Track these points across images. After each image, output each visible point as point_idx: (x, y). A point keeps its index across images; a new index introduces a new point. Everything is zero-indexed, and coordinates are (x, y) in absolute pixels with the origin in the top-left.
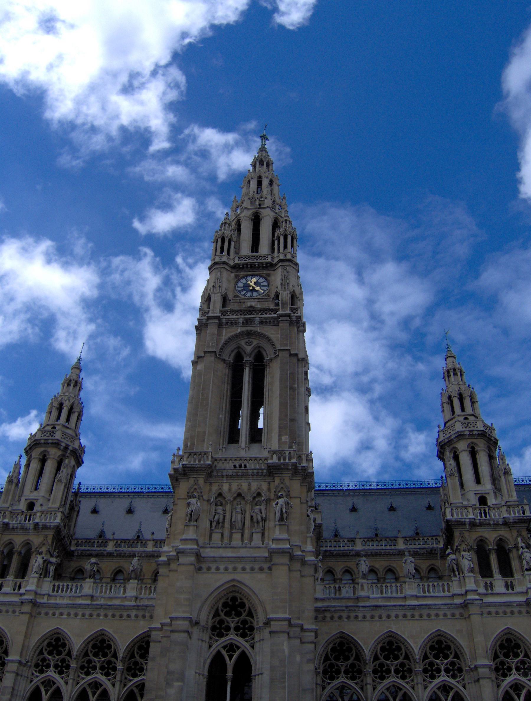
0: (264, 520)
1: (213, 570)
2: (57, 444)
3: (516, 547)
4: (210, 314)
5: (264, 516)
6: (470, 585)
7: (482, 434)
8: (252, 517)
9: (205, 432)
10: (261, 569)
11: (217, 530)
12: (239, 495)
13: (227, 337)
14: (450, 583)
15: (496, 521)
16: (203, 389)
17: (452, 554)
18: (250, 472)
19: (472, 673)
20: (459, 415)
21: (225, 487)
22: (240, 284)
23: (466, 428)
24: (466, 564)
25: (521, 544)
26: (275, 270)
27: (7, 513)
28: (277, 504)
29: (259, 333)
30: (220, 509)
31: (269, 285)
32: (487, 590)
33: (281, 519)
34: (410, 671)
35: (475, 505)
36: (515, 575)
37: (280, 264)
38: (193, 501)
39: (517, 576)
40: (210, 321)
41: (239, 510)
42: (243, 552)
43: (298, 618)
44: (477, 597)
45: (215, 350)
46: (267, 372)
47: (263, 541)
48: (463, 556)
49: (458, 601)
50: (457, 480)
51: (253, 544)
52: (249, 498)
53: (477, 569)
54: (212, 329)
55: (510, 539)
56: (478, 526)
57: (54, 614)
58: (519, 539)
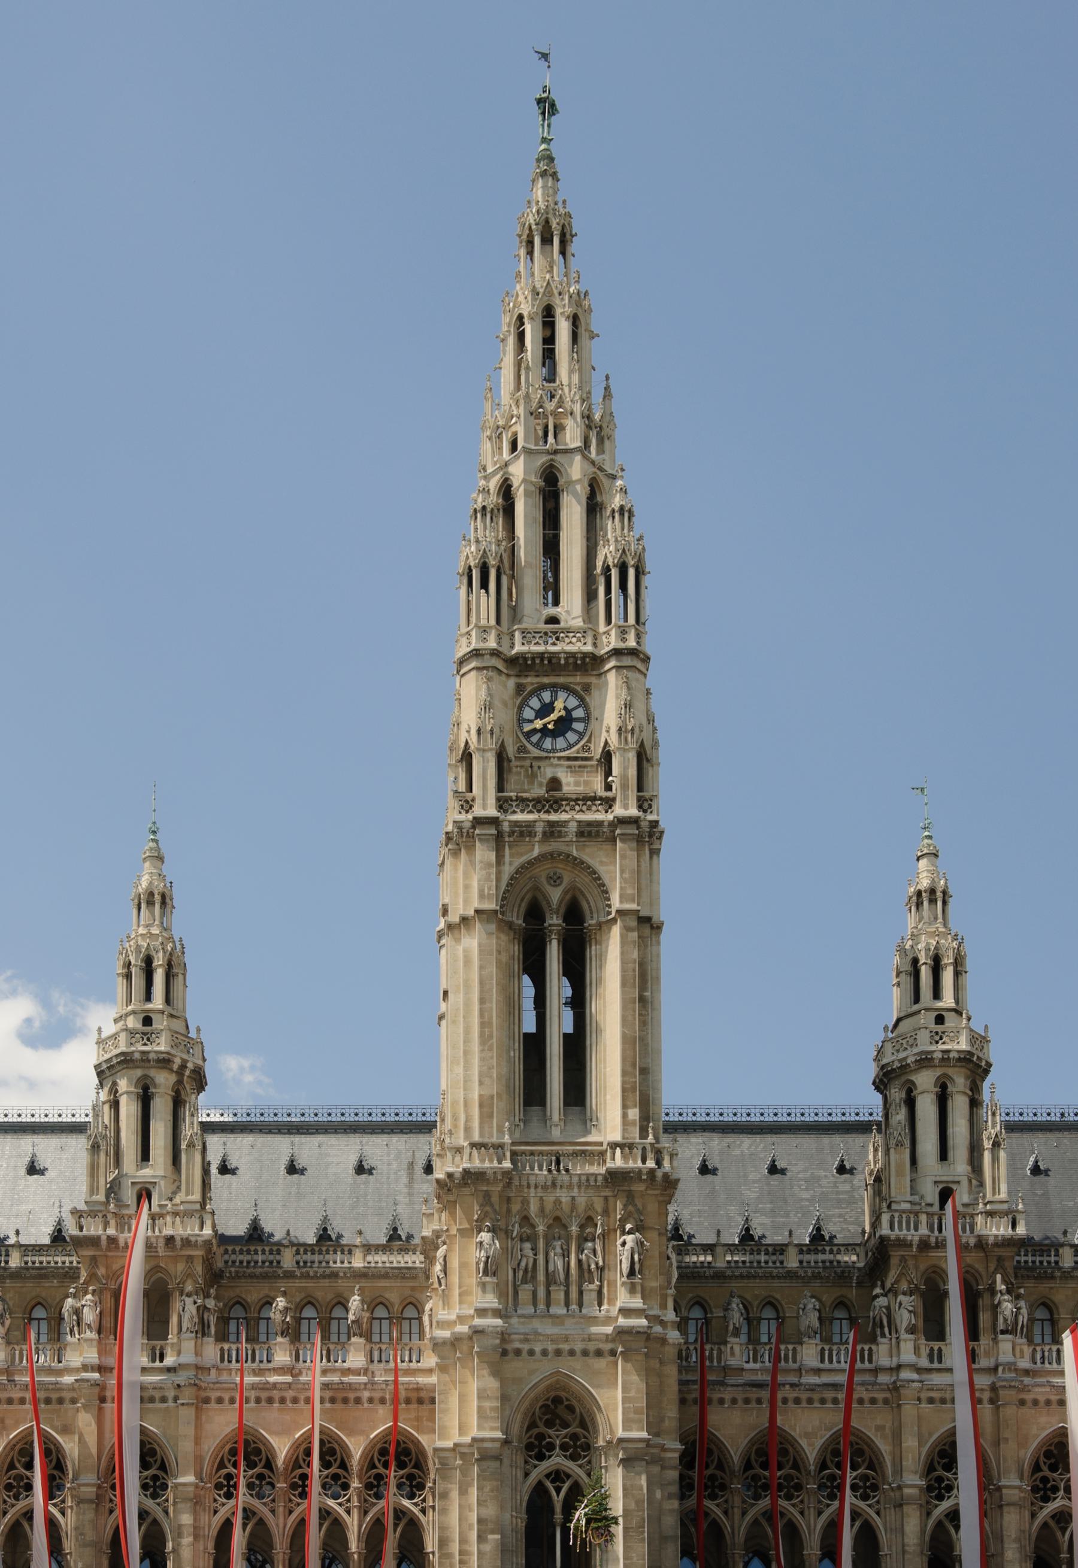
0: (602, 1269)
1: (524, 1353)
3: (992, 1290)
4: (478, 811)
5: (601, 1263)
6: (907, 1355)
7: (965, 1058)
8: (580, 1261)
9: (492, 1097)
10: (599, 1353)
11: (526, 1286)
12: (557, 1219)
13: (513, 869)
14: (874, 1347)
15: (964, 1240)
16: (482, 1001)
17: (882, 1295)
18: (575, 1180)
19: (892, 1494)
20: (926, 1010)
21: (533, 1208)
22: (528, 714)
23: (937, 1042)
24: (904, 1318)
25: (1001, 1286)
29: (575, 859)
30: (527, 1246)
32: (932, 1361)
34: (799, 1487)
35: (931, 1205)
36: (982, 1337)
38: (485, 1236)
39: (985, 1341)
41: (559, 1250)
43: (657, 1434)
44: (915, 1376)
45: (492, 905)
46: (592, 951)
47: (600, 1304)
48: (900, 1304)
49: (884, 1378)
50: (908, 1151)
51: (584, 1311)
52: (574, 1229)
53: (921, 1324)
54: (484, 853)
55: (984, 1273)
56: (933, 1248)
58: (999, 1277)
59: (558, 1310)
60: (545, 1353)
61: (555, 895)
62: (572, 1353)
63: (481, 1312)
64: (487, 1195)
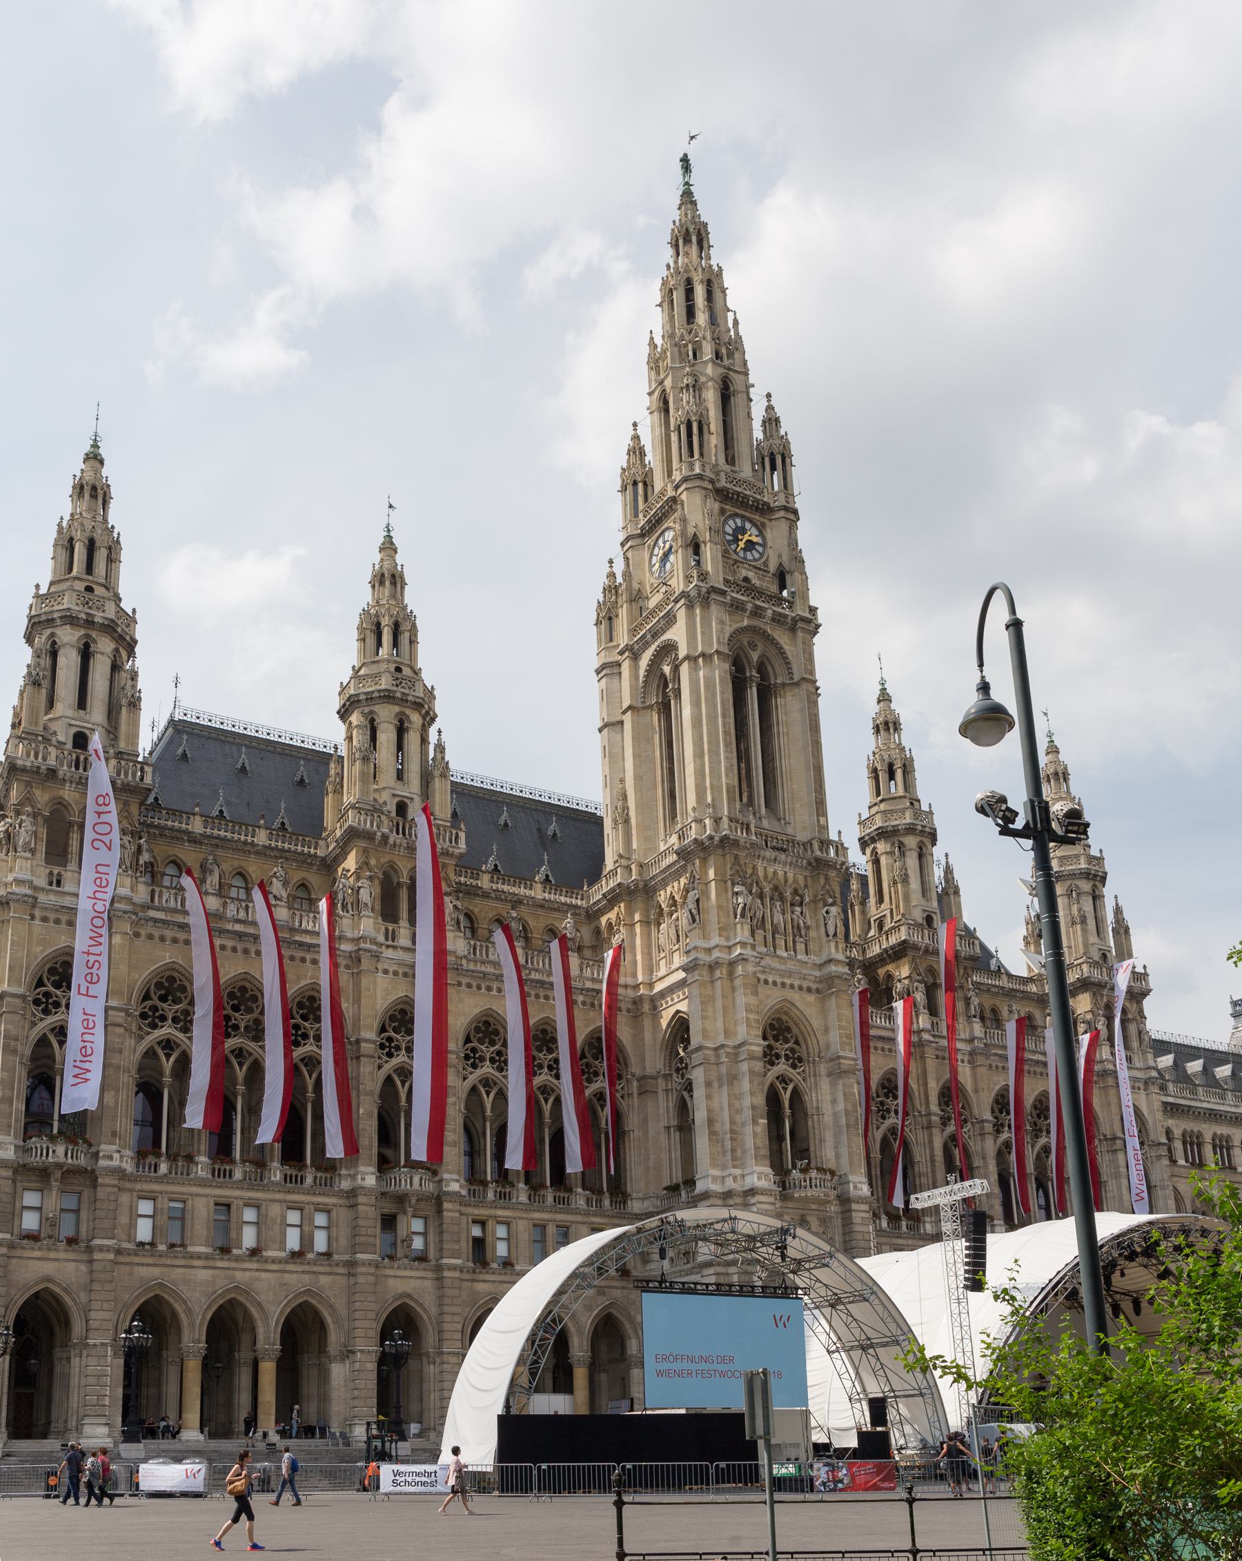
0: (807, 928)
2: (418, 706)
10: (809, 990)
13: (732, 630)
16: (724, 716)
18: (789, 860)
21: (761, 873)
26: (771, 520)
27: (383, 818)
28: (827, 912)
31: (764, 545)
33: (835, 935)
37: (782, 514)
40: (713, 596)
42: (790, 965)
52: (788, 894)
57: (479, 987)
59: (782, 953)
60: (775, 983)
61: (755, 656)
62: (792, 986)
63: (743, 944)
64: (736, 857)
